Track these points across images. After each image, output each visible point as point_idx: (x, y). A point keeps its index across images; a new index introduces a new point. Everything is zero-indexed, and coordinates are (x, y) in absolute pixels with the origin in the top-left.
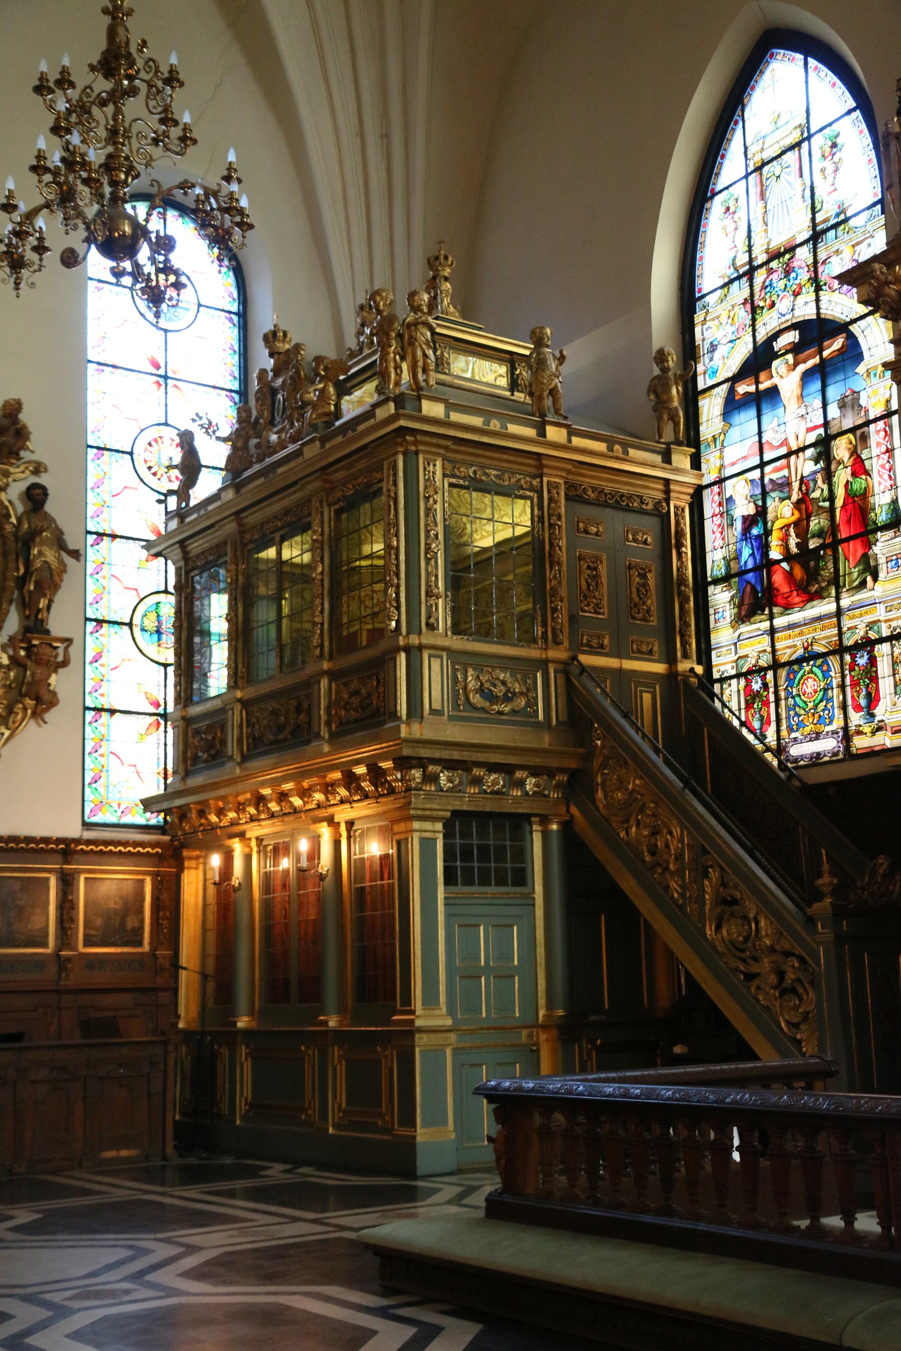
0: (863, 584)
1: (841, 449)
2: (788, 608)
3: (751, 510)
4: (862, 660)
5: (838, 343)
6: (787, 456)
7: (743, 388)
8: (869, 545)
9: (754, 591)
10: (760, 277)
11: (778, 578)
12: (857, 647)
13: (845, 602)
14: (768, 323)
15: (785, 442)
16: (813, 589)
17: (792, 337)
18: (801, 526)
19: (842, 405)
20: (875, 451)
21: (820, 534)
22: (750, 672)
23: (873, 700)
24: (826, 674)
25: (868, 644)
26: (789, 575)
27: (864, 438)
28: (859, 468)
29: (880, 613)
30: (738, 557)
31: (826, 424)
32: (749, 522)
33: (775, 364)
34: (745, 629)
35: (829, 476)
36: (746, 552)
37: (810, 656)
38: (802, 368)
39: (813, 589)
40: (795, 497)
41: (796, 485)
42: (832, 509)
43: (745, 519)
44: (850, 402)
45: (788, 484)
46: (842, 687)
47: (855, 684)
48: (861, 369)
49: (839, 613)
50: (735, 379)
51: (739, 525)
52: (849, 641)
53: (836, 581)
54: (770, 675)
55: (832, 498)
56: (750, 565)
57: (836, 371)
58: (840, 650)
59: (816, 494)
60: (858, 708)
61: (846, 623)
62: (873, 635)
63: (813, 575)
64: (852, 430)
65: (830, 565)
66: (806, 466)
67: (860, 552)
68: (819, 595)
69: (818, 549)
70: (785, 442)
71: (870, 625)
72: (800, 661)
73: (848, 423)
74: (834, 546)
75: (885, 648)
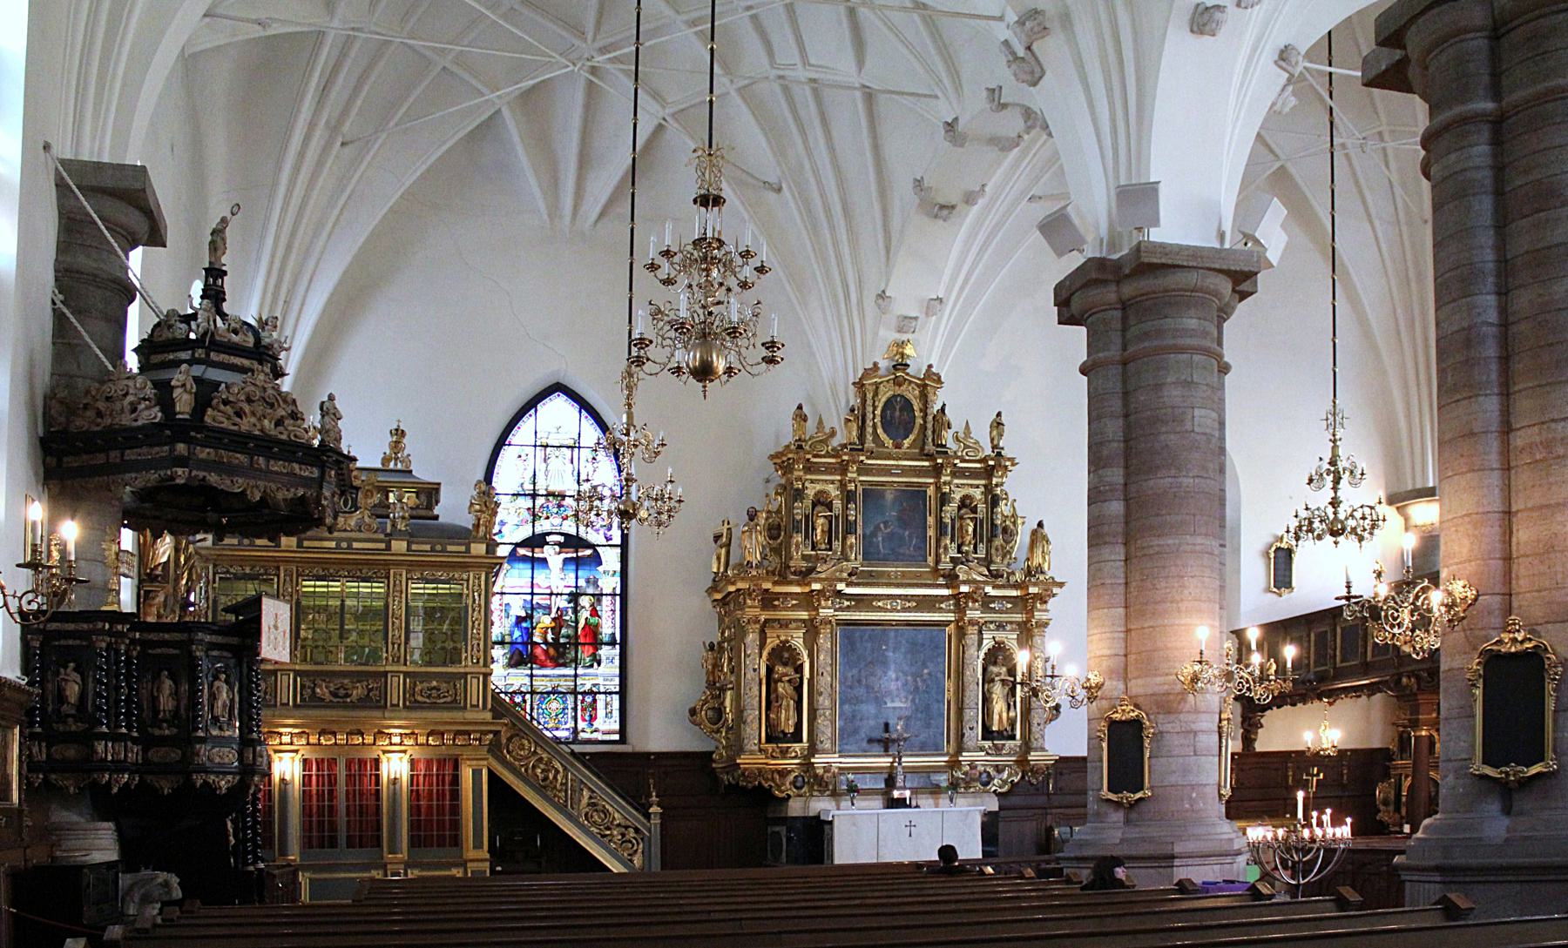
0: (592, 666)
1: (585, 601)
2: (543, 666)
3: (523, 614)
4: (589, 699)
5: (588, 552)
6: (551, 594)
7: (522, 551)
8: (596, 649)
9: (521, 654)
10: (540, 501)
11: (538, 651)
12: (584, 693)
13: (580, 671)
14: (543, 526)
15: (549, 587)
16: (561, 661)
17: (561, 539)
18: (556, 630)
19: (588, 581)
20: (604, 608)
21: (568, 637)
22: (514, 692)
23: (593, 718)
24: (564, 702)
25: (591, 692)
26: (546, 652)
27: (599, 601)
28: (594, 613)
29: (600, 681)
30: (511, 634)
31: (577, 587)
32: (519, 620)
33: (546, 547)
34: (512, 671)
35: (576, 612)
36: (517, 634)
37: (554, 692)
38: (564, 556)
39: (561, 661)
40: (553, 615)
41: (554, 610)
42: (576, 628)
43: (518, 617)
44: (594, 582)
45: (549, 607)
46: (575, 709)
47: (583, 709)
48: (600, 569)
49: (576, 676)
50: (517, 545)
51: (514, 619)
52: (580, 689)
53: (575, 660)
54: (528, 697)
55: (577, 622)
56: (520, 640)
57: (584, 564)
58: (575, 692)
59: (567, 618)
60: (584, 720)
61: (579, 681)
62: (595, 689)
63: (562, 655)
64: (593, 595)
65: (573, 653)
66: (562, 602)
67: (591, 650)
68: (564, 665)
69: (565, 644)
70: (549, 587)
71: (594, 685)
72: (548, 693)
73: (590, 591)
74: (577, 645)
75: (603, 696)
